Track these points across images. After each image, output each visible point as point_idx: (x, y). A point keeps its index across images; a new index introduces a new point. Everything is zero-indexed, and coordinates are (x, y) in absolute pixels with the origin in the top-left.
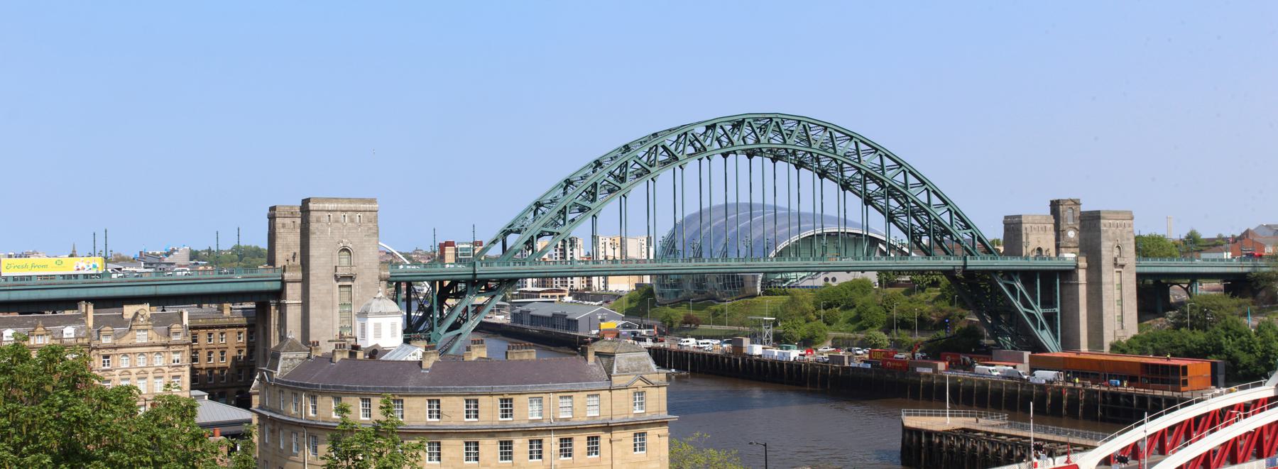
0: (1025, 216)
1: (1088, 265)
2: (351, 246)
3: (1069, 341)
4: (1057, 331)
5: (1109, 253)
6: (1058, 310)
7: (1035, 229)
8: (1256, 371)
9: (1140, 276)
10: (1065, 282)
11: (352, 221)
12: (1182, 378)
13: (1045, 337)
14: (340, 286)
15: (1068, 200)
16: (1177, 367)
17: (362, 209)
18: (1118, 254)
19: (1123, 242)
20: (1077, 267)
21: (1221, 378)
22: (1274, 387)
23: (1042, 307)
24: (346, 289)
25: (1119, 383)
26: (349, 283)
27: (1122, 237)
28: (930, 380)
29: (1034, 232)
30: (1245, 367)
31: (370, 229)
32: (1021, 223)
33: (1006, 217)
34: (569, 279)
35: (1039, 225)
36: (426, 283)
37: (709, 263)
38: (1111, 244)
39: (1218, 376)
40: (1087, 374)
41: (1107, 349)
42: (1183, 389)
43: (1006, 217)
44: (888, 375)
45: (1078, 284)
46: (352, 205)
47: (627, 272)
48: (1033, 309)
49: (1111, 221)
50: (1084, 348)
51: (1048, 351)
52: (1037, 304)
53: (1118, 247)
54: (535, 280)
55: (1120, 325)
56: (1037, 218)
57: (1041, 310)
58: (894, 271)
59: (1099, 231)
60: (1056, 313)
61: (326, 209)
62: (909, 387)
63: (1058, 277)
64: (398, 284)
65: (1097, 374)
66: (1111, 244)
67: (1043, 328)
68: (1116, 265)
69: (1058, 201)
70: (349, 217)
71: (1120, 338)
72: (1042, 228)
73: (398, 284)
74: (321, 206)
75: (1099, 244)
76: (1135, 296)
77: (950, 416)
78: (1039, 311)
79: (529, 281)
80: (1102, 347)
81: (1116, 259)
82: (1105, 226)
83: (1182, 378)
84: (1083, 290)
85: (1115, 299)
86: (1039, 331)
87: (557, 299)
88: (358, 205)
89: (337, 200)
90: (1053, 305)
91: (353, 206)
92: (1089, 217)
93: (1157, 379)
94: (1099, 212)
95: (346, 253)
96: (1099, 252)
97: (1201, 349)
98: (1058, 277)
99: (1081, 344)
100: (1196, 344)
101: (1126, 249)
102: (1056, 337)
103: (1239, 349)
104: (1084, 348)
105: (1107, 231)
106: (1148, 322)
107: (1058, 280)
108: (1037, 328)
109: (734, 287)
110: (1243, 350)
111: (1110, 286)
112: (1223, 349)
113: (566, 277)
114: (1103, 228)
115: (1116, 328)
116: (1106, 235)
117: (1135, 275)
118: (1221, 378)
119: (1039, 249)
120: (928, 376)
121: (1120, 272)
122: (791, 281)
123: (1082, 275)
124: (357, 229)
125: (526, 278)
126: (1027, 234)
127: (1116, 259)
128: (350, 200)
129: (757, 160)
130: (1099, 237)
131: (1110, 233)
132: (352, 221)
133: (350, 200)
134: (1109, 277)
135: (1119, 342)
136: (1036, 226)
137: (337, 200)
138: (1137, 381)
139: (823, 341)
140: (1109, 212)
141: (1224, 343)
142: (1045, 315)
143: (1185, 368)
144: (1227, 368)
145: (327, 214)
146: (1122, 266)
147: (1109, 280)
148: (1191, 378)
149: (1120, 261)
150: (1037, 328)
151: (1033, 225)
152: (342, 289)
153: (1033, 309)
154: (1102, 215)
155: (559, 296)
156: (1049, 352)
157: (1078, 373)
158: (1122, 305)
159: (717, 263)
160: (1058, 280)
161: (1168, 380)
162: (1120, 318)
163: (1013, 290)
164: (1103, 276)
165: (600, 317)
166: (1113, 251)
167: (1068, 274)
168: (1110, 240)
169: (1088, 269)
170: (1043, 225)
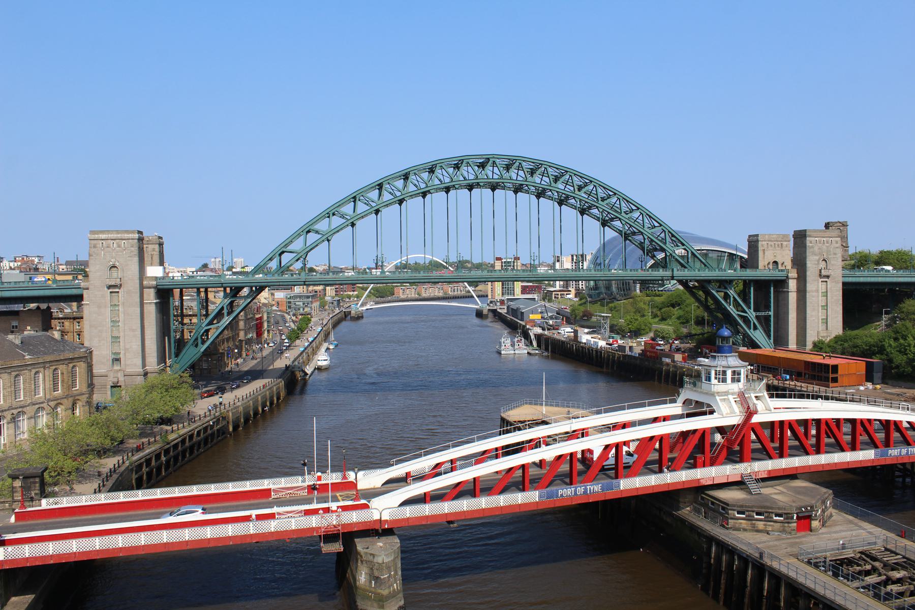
0: (761, 235)
1: (798, 276)
2: (118, 264)
3: (780, 340)
4: (770, 331)
5: (815, 266)
6: (771, 313)
7: (771, 245)
8: (904, 371)
9: (844, 284)
10: (781, 290)
11: (119, 246)
12: (831, 376)
13: (758, 335)
14: (111, 292)
15: (836, 223)
16: (827, 366)
17: (126, 238)
18: (825, 266)
19: (830, 257)
20: (787, 277)
21: (877, 376)
22: (681, 405)
23: (754, 311)
24: (116, 294)
25: (788, 377)
26: (117, 290)
27: (828, 252)
28: (668, 368)
29: (770, 248)
30: (897, 367)
31: (132, 251)
32: (758, 241)
33: (750, 236)
34: (580, 282)
35: (776, 243)
36: (465, 283)
37: (425, 275)
38: (817, 258)
39: (875, 374)
40: (771, 368)
41: (809, 346)
42: (831, 385)
43: (750, 236)
44: (646, 363)
45: (788, 292)
46: (119, 235)
47: (350, 282)
48: (746, 313)
49: (816, 239)
50: (792, 345)
51: (760, 347)
52: (750, 308)
53: (824, 260)
54: (562, 283)
55: (824, 327)
56: (774, 236)
57: (754, 314)
58: (634, 280)
59: (805, 247)
60: (770, 316)
61: (100, 238)
62: (657, 372)
63: (772, 285)
64: (198, 289)
65: (777, 369)
66: (817, 258)
67: (755, 328)
68: (820, 275)
69: (828, 223)
70: (117, 243)
71: (823, 337)
72: (778, 245)
73: (198, 289)
74: (131, 236)
75: (805, 258)
76: (841, 302)
77: (546, 405)
78: (752, 314)
79: (557, 283)
80: (805, 345)
81: (820, 270)
82: (811, 242)
83: (831, 376)
84: (793, 298)
85: (820, 305)
86: (752, 330)
87: (559, 296)
88: (123, 235)
89: (108, 232)
90: (768, 308)
91: (119, 236)
92: (800, 235)
93: (815, 376)
94: (805, 231)
95: (113, 269)
96: (805, 264)
97: (869, 350)
98: (772, 285)
99: (790, 342)
100: (866, 345)
101: (832, 262)
102: (769, 337)
103: (897, 351)
104: (792, 345)
105: (812, 247)
106: (878, 323)
107: (772, 288)
108: (750, 328)
109: (624, 290)
110: (900, 351)
111: (814, 294)
112: (885, 350)
113: (578, 281)
114: (808, 244)
115: (820, 329)
116: (812, 250)
117: (840, 285)
118: (877, 376)
119: (775, 263)
120: (668, 364)
121: (826, 281)
122: (667, 286)
123: (792, 285)
124: (122, 252)
125: (556, 281)
126: (764, 250)
127: (820, 272)
128: (118, 232)
129: (475, 191)
130: (805, 252)
131: (816, 249)
132: (119, 246)
133: (118, 232)
134: (814, 285)
135: (822, 342)
136: (772, 243)
137: (108, 232)
138: (802, 376)
139: (647, 333)
140: (815, 231)
141: (887, 345)
142: (757, 317)
143: (835, 368)
144: (884, 367)
145: (101, 242)
146: (828, 277)
147: (814, 289)
148: (843, 375)
149: (823, 273)
150: (750, 328)
151: (770, 243)
152: (113, 294)
153: (746, 313)
154: (807, 233)
155: (561, 294)
156: (760, 348)
157: (765, 367)
158: (827, 310)
159: (328, 277)
160: (772, 288)
161: (821, 377)
162: (825, 321)
163: (727, 296)
164: (808, 285)
165: (539, 311)
166: (818, 264)
167: (781, 284)
168: (815, 255)
169: (798, 279)
170: (779, 243)
